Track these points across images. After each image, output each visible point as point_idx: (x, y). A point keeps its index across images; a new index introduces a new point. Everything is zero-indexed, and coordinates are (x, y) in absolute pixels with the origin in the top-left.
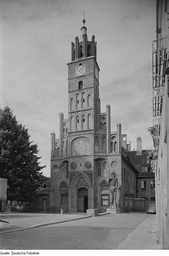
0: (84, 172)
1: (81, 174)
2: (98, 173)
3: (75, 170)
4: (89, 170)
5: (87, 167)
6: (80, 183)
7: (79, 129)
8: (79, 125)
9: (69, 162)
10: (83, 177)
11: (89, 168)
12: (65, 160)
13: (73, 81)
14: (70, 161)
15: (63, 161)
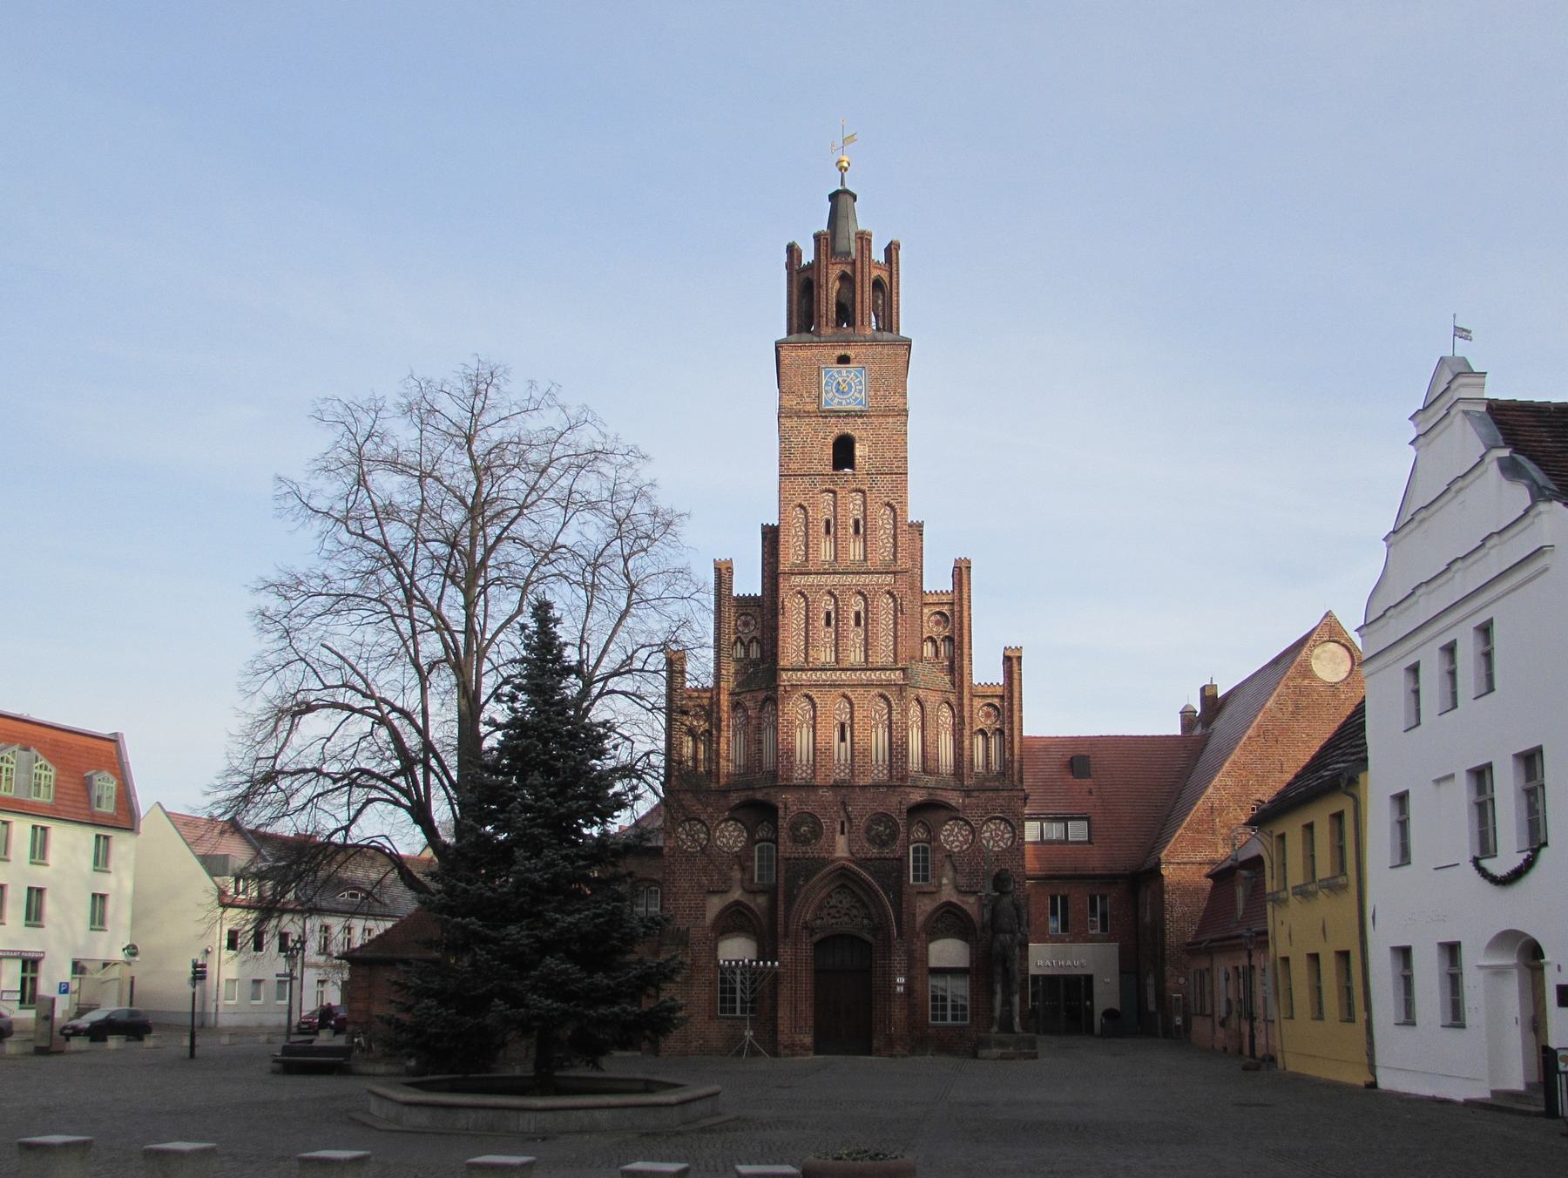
0: (864, 862)
1: (844, 873)
2: (916, 869)
3: (811, 851)
4: (887, 853)
5: (871, 841)
6: (833, 911)
7: (826, 656)
8: (824, 635)
9: (781, 813)
10: (850, 885)
11: (883, 844)
12: (759, 796)
13: (805, 427)
14: (786, 808)
15: (735, 798)
